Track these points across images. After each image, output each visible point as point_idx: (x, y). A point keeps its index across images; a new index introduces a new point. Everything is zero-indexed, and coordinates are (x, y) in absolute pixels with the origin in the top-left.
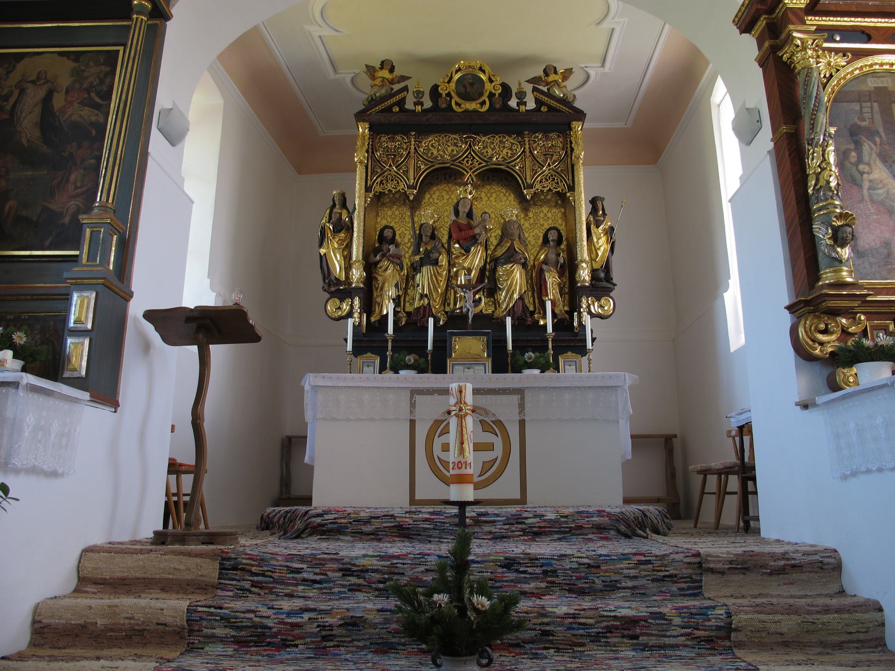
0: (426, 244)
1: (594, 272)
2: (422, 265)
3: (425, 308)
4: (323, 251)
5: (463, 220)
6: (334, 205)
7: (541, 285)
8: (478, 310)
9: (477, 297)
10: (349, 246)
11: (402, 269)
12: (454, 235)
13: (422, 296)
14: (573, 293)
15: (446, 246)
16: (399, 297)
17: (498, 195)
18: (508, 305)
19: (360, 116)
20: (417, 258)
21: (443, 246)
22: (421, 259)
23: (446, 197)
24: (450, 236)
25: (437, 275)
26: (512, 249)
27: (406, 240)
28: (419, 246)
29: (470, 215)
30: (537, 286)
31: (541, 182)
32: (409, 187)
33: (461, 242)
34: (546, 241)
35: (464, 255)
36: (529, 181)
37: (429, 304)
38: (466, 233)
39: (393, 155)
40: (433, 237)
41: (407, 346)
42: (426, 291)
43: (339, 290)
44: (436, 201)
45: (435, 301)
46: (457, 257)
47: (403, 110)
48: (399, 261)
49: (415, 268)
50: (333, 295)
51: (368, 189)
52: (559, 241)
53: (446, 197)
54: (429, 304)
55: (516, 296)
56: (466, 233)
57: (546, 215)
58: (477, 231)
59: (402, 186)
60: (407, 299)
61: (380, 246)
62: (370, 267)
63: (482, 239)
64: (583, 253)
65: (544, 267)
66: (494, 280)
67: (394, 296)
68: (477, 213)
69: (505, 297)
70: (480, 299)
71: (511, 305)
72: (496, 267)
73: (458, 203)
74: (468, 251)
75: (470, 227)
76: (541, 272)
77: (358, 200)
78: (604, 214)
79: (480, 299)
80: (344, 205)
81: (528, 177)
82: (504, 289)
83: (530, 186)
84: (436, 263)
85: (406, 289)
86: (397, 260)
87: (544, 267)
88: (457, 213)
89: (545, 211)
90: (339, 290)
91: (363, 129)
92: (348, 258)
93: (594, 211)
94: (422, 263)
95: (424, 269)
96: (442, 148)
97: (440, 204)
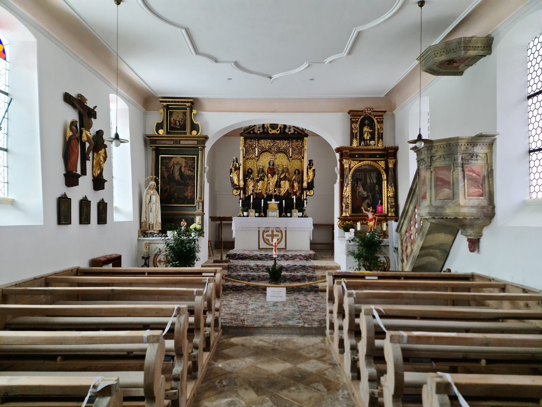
1: (308, 183)
4: (231, 176)
6: (234, 162)
10: (239, 174)
14: (302, 189)
19: (241, 135)
25: (264, 184)
28: (259, 174)
29: (273, 165)
30: (292, 186)
34: (295, 173)
39: (251, 146)
40: (263, 171)
41: (256, 204)
43: (236, 187)
47: (254, 133)
49: (258, 181)
50: (235, 189)
51: (244, 157)
52: (299, 173)
56: (272, 171)
59: (253, 156)
61: (247, 174)
62: (245, 181)
64: (305, 178)
66: (280, 185)
68: (276, 164)
74: (273, 177)
75: (274, 169)
76: (293, 183)
77: (241, 162)
78: (313, 165)
80: (237, 162)
83: (291, 157)
84: (263, 180)
86: (253, 179)
88: (270, 164)
90: (236, 187)
91: (242, 138)
92: (239, 178)
93: (310, 164)
94: (260, 180)
96: (266, 143)
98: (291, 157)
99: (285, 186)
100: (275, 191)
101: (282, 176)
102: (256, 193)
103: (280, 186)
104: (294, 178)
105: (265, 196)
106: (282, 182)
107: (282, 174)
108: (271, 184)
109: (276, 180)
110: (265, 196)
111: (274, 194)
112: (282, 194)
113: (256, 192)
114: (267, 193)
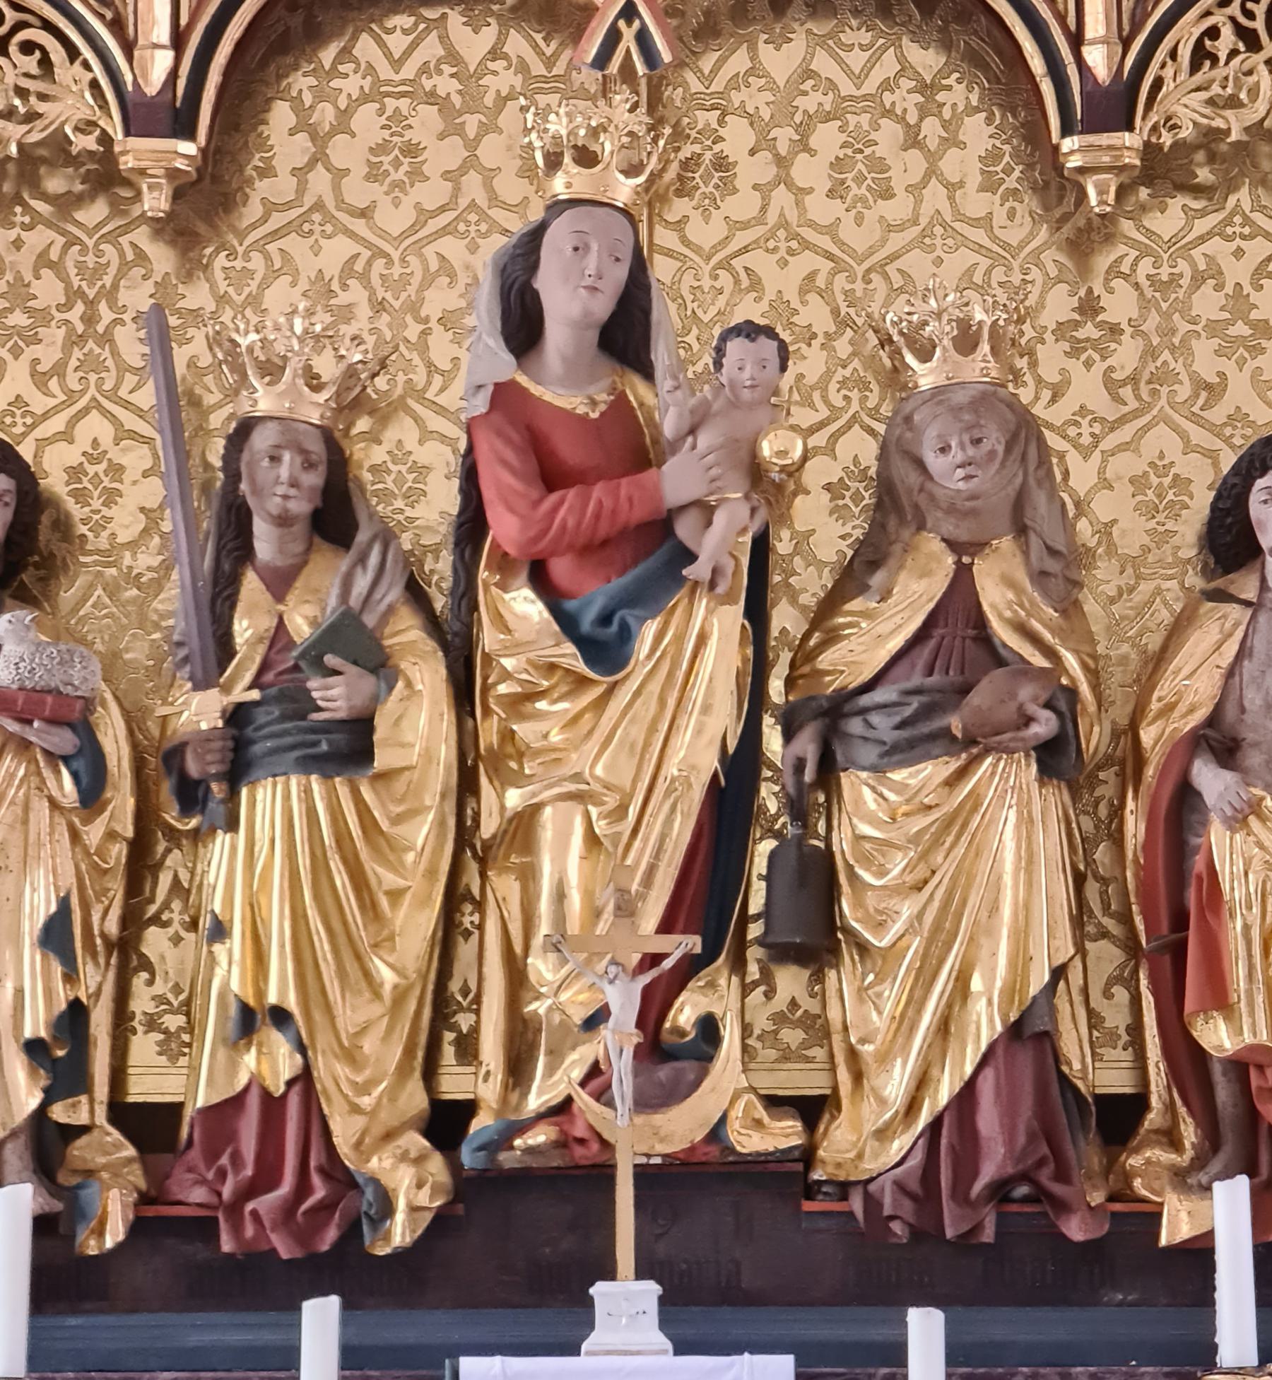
0: (280, 583)
2: (238, 770)
3: (272, 1106)
5: (566, 386)
7: (1180, 921)
8: (680, 1128)
9: (685, 1013)
11: (92, 794)
12: (505, 527)
13: (249, 1021)
15: (441, 567)
16: (74, 1019)
17: (859, 143)
18: (922, 1083)
20: (198, 711)
21: (416, 593)
22: (237, 716)
23: (443, 156)
24: (471, 526)
26: (958, 611)
27: (125, 521)
29: (625, 335)
31: (1201, 55)
32: (144, 116)
33: (561, 569)
35: (582, 682)
36: (1097, 58)
37: (305, 1078)
38: (598, 519)
40: (334, 516)
42: (280, 989)
44: (357, 191)
45: (351, 1056)
46: (521, 702)
48: (65, 740)
49: (192, 788)
53: (443, 156)
54: (305, 1078)
55: (985, 1022)
56: (598, 519)
57: (1239, 303)
58: (678, 480)
59: (71, 104)
60: (142, 1002)
63: (719, 542)
65: (1211, 780)
66: (815, 879)
67: (36, 1024)
69: (905, 1022)
70: (709, 1028)
71: (944, 1091)
72: (828, 769)
73: (535, 236)
74: (605, 649)
76: (1182, 808)
79: (709, 1028)
81: (1095, 25)
82: (894, 952)
83: (1114, 106)
84: (351, 747)
85: (126, 952)
87: (1211, 780)
88: (523, 325)
89: (1238, 273)
95: (269, 802)
97: (395, 219)
98: (1114, 106)
99: (968, 897)
100: (673, 1059)
101: (871, 640)
102: (150, 1127)
103: (815, 931)
104: (1192, 685)
105: (410, 1188)
106: (874, 809)
107: (860, 571)
108: (562, 856)
109: (696, 755)
110: (410, 1188)
111: (640, 1138)
112: (869, 1142)
113: (151, 1082)
114: (445, 1124)
